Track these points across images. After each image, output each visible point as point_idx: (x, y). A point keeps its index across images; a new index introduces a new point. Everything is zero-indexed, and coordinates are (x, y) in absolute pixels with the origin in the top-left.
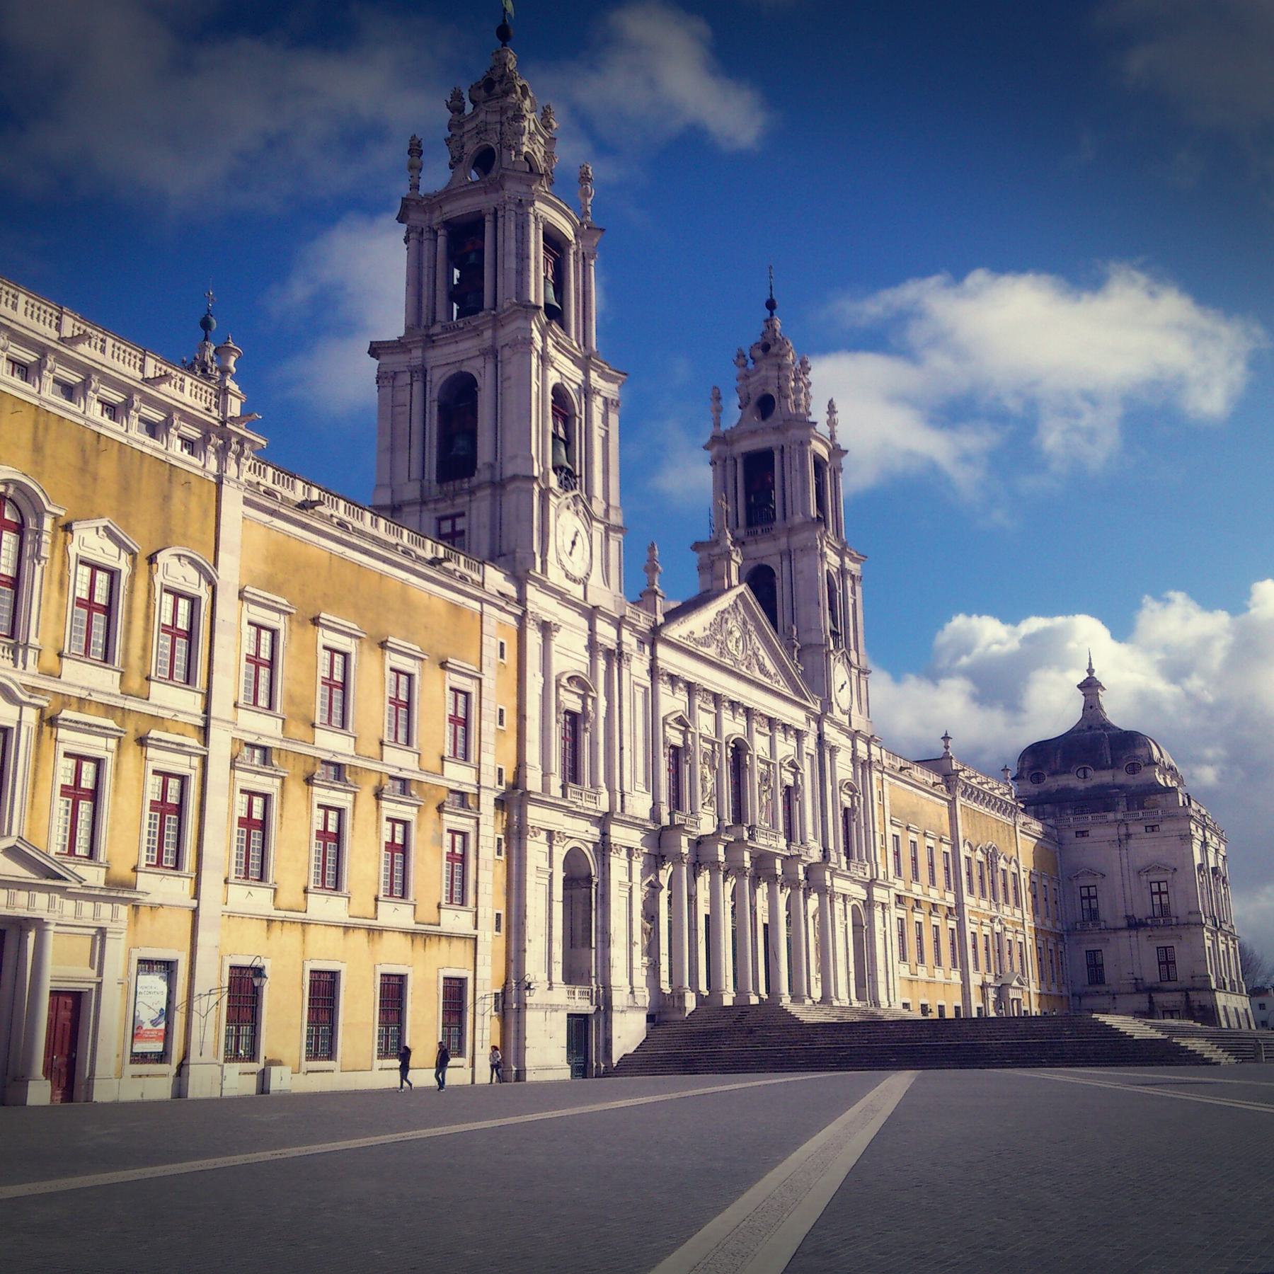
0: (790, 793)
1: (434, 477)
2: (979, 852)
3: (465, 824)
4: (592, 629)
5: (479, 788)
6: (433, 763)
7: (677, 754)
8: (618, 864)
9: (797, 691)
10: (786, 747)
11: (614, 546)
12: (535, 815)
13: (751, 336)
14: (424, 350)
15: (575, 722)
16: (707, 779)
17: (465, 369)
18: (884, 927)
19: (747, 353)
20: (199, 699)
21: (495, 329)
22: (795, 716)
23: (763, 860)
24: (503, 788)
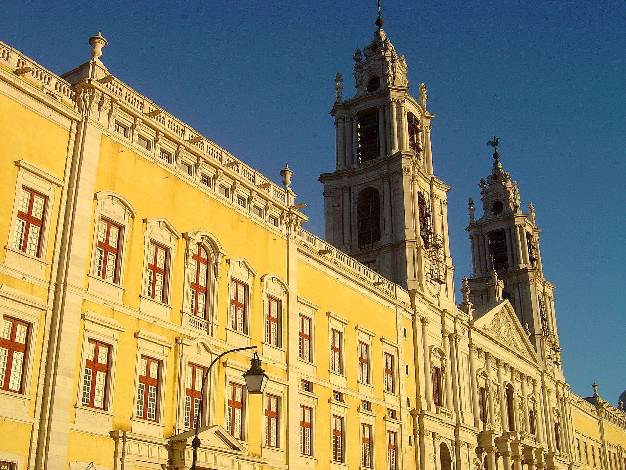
0: (532, 414)
1: (356, 241)
2: (613, 448)
3: (395, 428)
4: (442, 323)
5: (400, 408)
6: (380, 395)
7: (483, 391)
8: (463, 450)
10: (528, 390)
12: (427, 423)
13: (489, 172)
14: (349, 177)
15: (438, 373)
16: (497, 408)
19: (486, 180)
20: (284, 355)
21: (388, 165)
22: (530, 371)
23: (527, 449)
24: (410, 408)
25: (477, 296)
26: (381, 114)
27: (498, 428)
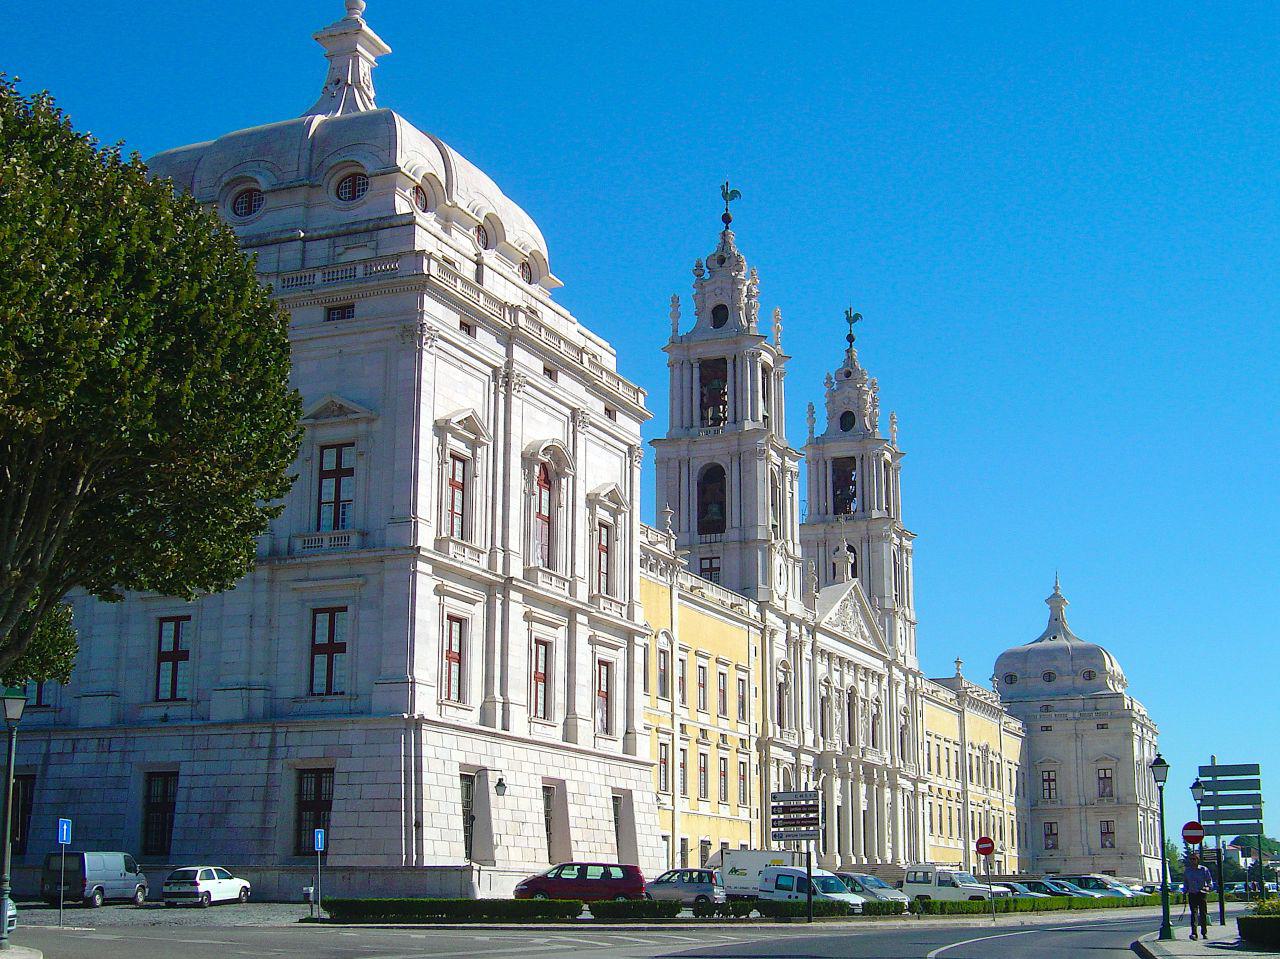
0: (876, 717)
3: (744, 759)
9: (880, 647)
11: (797, 569)
13: (838, 362)
16: (838, 716)
17: (716, 461)
18: (923, 810)
19: (833, 376)
22: (877, 665)
23: (869, 768)
25: (821, 574)
26: (730, 366)
27: (837, 743)
